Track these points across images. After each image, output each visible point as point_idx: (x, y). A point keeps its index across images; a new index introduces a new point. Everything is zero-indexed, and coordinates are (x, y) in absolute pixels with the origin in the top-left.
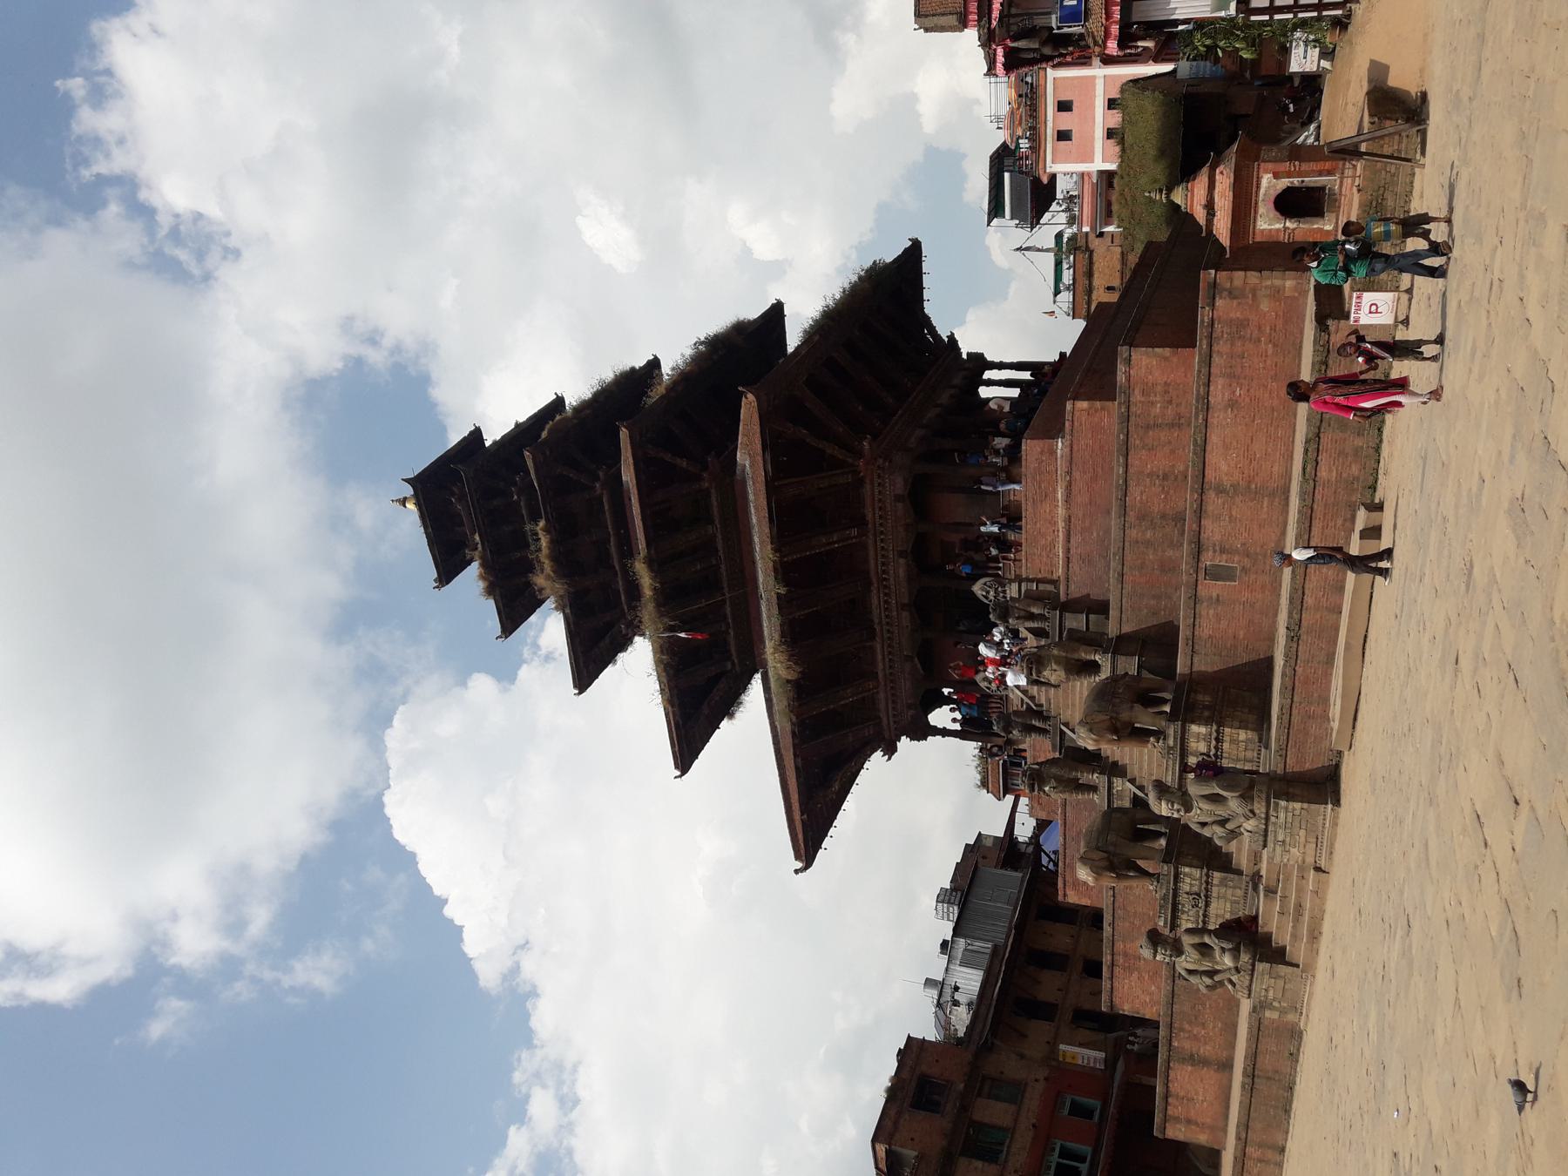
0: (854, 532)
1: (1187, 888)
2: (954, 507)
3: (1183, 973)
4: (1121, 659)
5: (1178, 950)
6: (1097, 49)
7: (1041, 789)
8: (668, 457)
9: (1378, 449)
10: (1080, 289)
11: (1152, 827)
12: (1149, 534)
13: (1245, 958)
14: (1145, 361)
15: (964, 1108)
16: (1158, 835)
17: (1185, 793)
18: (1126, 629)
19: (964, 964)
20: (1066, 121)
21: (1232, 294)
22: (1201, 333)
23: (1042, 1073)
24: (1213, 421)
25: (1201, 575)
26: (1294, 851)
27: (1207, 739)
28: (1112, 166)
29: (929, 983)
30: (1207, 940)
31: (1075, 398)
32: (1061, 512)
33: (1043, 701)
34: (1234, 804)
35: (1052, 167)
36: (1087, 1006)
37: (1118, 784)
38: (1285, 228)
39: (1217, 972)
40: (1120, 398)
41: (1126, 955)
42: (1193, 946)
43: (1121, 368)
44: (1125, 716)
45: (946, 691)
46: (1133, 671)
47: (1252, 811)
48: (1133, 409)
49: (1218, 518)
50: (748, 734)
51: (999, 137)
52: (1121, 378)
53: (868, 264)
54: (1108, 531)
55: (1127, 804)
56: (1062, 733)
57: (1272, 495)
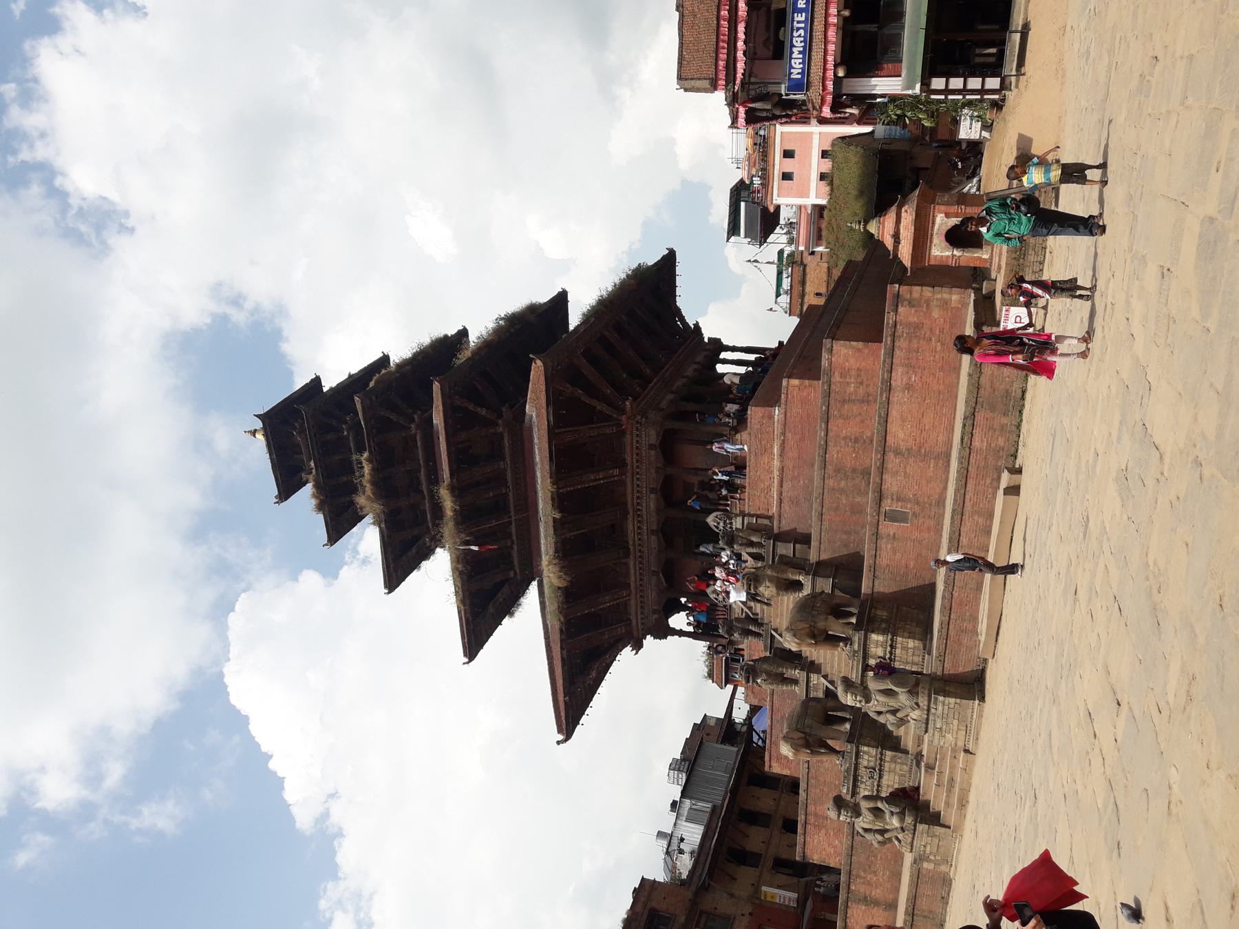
0: (616, 472)
1: (865, 763)
3: (861, 831)
4: (819, 581)
5: (858, 813)
6: (815, 113)
7: (754, 681)
8: (471, 407)
9: (1019, 426)
10: (795, 293)
11: (839, 714)
12: (843, 484)
13: (909, 820)
14: (844, 351)
16: (844, 720)
17: (866, 688)
18: (824, 557)
19: (688, 820)
20: (789, 165)
21: (911, 304)
22: (887, 332)
23: (748, 909)
24: (894, 399)
25: (882, 518)
26: (949, 736)
27: (883, 645)
28: (823, 202)
29: (660, 834)
30: (880, 805)
32: (776, 463)
33: (758, 611)
34: (903, 698)
35: (777, 200)
36: (784, 856)
37: (814, 678)
38: (953, 256)
39: (886, 831)
40: (824, 378)
41: (816, 815)
42: (870, 810)
43: (825, 355)
44: (821, 625)
45: (683, 600)
46: (828, 590)
47: (917, 704)
48: (833, 387)
50: (525, 630)
51: (737, 175)
52: (825, 363)
53: (635, 266)
54: (812, 480)
55: (821, 695)
56: (772, 636)
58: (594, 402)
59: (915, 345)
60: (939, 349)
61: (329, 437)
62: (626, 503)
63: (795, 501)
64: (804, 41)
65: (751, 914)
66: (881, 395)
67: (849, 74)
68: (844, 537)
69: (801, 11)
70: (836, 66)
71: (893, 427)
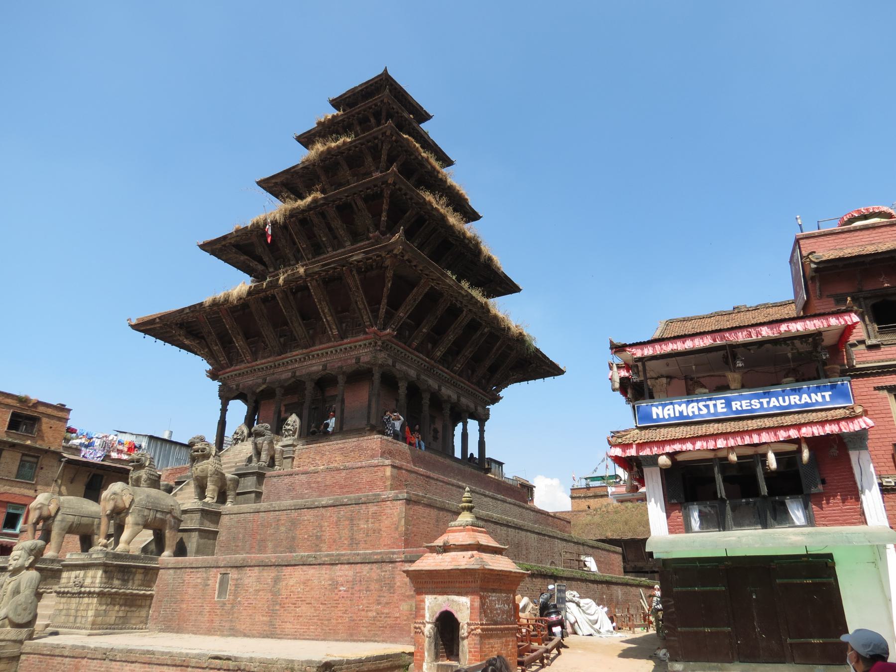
0: (335, 332)
2: (358, 399)
8: (385, 207)
12: (283, 529)
15: (13, 446)
24: (324, 570)
25: (223, 571)
31: (393, 466)
43: (391, 494)
44: (130, 520)
48: (364, 507)
49: (258, 580)
57: (271, 624)
58: (384, 301)
59: (374, 586)
62: (314, 345)
63: (291, 488)
64: (694, 416)
66: (327, 556)
67: (666, 473)
68: (241, 536)
69: (728, 404)
70: (668, 454)
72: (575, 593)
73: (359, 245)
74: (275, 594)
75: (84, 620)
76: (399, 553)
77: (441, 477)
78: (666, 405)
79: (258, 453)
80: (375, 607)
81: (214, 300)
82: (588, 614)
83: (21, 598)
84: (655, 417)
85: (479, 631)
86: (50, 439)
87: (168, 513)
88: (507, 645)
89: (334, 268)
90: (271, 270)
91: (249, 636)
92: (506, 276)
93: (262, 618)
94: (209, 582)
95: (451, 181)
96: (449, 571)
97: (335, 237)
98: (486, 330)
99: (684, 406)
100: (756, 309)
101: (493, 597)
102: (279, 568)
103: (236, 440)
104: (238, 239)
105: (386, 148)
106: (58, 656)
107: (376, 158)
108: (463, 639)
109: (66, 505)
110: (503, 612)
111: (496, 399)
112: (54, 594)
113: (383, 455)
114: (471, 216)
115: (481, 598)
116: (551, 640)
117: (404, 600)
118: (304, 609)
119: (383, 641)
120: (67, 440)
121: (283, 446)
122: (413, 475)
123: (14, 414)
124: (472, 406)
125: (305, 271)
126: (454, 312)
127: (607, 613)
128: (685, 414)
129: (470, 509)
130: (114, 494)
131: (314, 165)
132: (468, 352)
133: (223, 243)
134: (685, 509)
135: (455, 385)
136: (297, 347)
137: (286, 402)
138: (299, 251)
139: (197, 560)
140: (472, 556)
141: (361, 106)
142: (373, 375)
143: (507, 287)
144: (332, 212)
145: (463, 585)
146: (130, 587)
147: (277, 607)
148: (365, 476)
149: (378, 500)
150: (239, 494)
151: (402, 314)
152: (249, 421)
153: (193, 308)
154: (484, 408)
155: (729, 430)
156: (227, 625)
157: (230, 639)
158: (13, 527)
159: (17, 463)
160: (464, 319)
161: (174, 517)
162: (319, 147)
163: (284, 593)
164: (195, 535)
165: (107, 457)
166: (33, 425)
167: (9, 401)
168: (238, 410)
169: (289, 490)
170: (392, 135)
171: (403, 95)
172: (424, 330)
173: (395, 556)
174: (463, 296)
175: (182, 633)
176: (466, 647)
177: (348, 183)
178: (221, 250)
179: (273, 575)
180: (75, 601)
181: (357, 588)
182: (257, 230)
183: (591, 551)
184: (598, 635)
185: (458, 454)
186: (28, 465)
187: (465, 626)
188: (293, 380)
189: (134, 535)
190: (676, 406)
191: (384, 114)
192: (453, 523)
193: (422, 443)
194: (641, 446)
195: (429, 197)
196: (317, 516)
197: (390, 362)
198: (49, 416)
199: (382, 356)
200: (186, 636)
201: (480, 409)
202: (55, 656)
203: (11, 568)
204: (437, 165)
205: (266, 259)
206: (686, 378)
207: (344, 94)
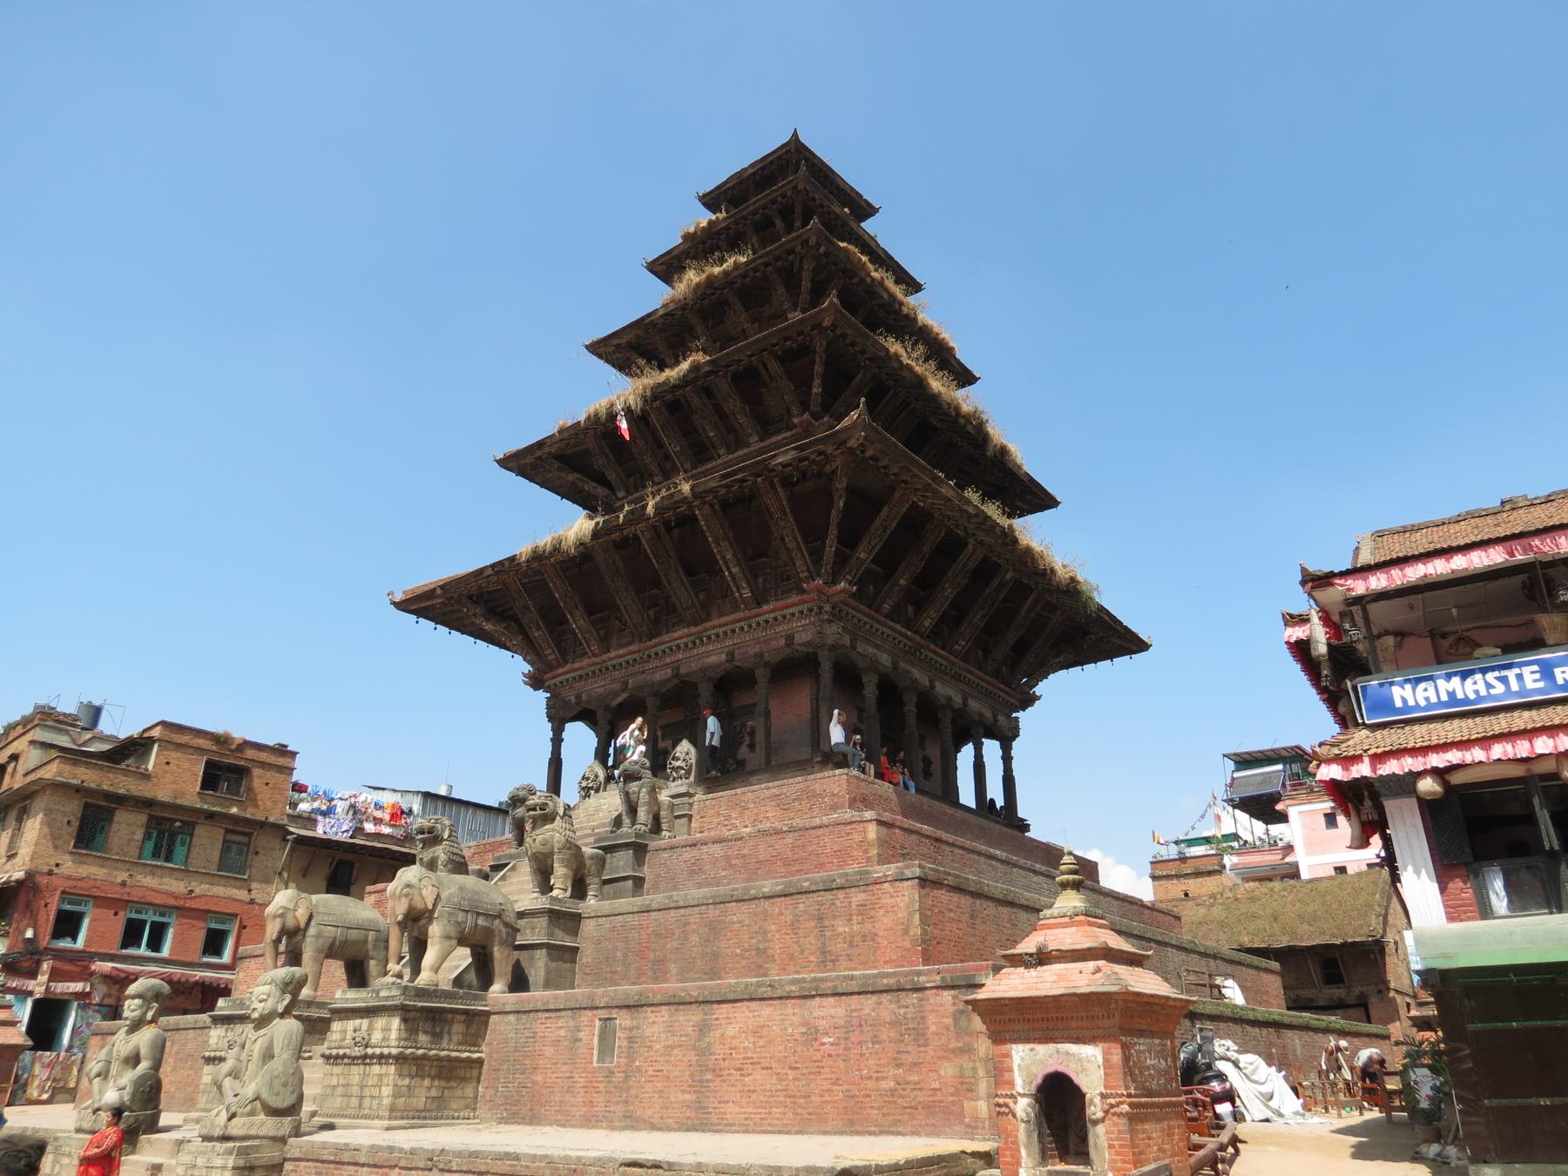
0: (747, 593)
12: (694, 939)
14: (901, 902)
15: (211, 816)
21: (957, 1016)
24: (790, 1008)
25: (604, 1014)
28: (1305, 875)
29: (96, 712)
30: (144, 1065)
31: (880, 823)
35: (1293, 812)
43: (891, 869)
44: (435, 930)
48: (841, 894)
49: (670, 1028)
57: (699, 1106)
58: (833, 532)
59: (886, 1034)
60: (884, 1085)
61: (778, 222)
62: (708, 618)
64: (1479, 699)
65: (252, 902)
66: (794, 982)
67: (1430, 810)
68: (619, 954)
69: (1547, 671)
70: (1436, 772)
71: (743, 1012)
72: (1229, 1043)
73: (774, 439)
74: (701, 1053)
75: (375, 1103)
76: (929, 973)
77: (960, 840)
78: (1418, 681)
79: (632, 810)
80: (893, 1072)
81: (535, 551)
82: (1256, 1082)
83: (277, 1065)
84: (1399, 704)
85: (1125, 1108)
86: (267, 804)
87: (495, 917)
88: (1170, 1135)
89: (743, 480)
90: (621, 494)
91: (660, 1129)
92: (1032, 480)
93: (681, 1097)
94: (581, 1035)
95: (924, 317)
96: (1056, 998)
97: (731, 430)
98: (1008, 577)
99: (1456, 680)
100: (1548, 500)
101: (1142, 1044)
102: (707, 1007)
103: (586, 792)
104: (563, 445)
105: (808, 266)
106: (349, 1163)
107: (792, 285)
108: (1095, 1123)
109: (322, 909)
110: (1159, 1072)
111: (1028, 701)
112: (321, 1061)
113: (852, 804)
114: (965, 378)
115: (1125, 1047)
116: (1222, 1127)
117: (946, 1058)
118: (757, 1078)
119: (913, 1133)
120: (294, 805)
121: (673, 797)
122: (913, 837)
123: (209, 764)
124: (988, 714)
125: (692, 489)
126: (951, 547)
127: (1286, 1078)
128: (1460, 695)
129: (1076, 886)
130: (408, 886)
131: (683, 309)
132: (978, 617)
133: (538, 453)
134: (1476, 876)
135: (957, 678)
136: (681, 622)
137: (662, 722)
138: (667, 457)
139: (556, 997)
140: (1098, 970)
141: (756, 201)
142: (819, 664)
143: (1036, 499)
144: (723, 386)
145: (1085, 1023)
146: (445, 1045)
147: (709, 1076)
148: (830, 843)
149: (865, 882)
150: (606, 882)
151: (863, 554)
152: (601, 755)
153: (498, 567)
154: (1009, 716)
155: (1557, 721)
156: (619, 1109)
157: (628, 1134)
158: (218, 952)
159: (219, 845)
160: (970, 557)
161: (507, 925)
162: (692, 277)
163: (717, 1048)
164: (541, 954)
165: (359, 831)
166: (239, 782)
167: (200, 742)
168: (580, 739)
169: (692, 872)
170: (818, 244)
171: (826, 176)
172: (902, 582)
173: (923, 978)
174: (970, 516)
175: (539, 1124)
176: (1101, 1137)
177: (744, 335)
178: (534, 466)
179: (695, 1019)
180: (357, 1070)
181: (854, 1038)
182: (601, 427)
183: (1229, 968)
184: (1281, 1121)
185: (967, 797)
186: (234, 848)
187: (1097, 1100)
188: (675, 681)
189: (444, 957)
190: (1441, 683)
191: (798, 210)
192: (1047, 912)
193: (912, 784)
194: (1378, 759)
195: (894, 347)
196: (755, 914)
197: (847, 640)
198: (264, 765)
199: (833, 632)
200: (548, 1129)
201: (1002, 719)
202: (343, 1163)
203: (255, 1015)
204: (897, 291)
205: (611, 476)
206: (1432, 634)
207: (726, 183)
